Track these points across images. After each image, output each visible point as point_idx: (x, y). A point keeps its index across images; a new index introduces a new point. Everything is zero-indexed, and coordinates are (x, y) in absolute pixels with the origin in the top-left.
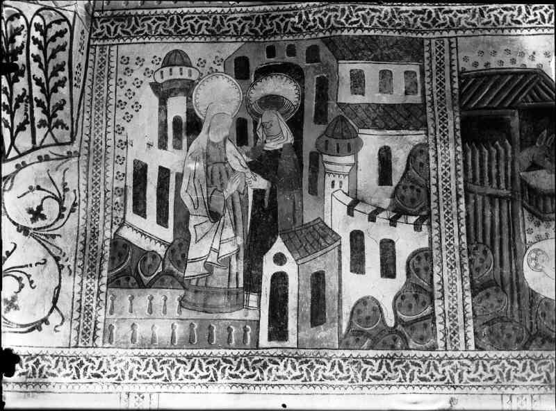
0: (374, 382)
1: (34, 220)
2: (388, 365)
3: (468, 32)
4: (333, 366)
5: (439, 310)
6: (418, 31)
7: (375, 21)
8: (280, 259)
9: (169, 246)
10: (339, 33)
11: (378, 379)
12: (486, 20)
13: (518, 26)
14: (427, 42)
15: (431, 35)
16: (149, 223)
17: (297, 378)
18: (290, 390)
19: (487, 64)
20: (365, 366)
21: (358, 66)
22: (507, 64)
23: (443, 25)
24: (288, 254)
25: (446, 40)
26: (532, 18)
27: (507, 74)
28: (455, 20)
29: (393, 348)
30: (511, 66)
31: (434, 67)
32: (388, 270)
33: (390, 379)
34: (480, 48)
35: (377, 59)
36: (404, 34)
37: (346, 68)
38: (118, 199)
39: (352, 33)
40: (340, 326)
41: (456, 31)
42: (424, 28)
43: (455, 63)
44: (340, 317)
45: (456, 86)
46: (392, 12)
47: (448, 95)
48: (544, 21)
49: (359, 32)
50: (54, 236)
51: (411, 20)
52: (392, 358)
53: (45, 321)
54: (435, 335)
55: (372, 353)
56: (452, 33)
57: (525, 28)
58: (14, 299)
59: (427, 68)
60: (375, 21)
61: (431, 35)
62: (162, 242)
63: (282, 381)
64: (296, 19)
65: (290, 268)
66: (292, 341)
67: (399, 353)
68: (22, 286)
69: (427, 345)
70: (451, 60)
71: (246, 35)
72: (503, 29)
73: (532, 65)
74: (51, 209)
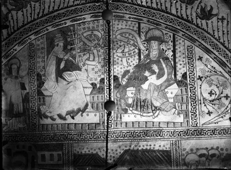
3: (76, 142)
6: (62, 141)
7: (48, 139)
10: (37, 143)
12: (82, 138)
13: (91, 140)
14: (64, 144)
15: (65, 142)
19: (81, 152)
21: (43, 153)
22: (87, 152)
23: (69, 139)
25: (70, 144)
26: (95, 137)
27: (87, 155)
28: (73, 137)
30: (88, 153)
31: (66, 152)
34: (80, 147)
35: (49, 151)
36: (57, 142)
37: (40, 154)
39: (41, 143)
41: (73, 141)
42: (64, 140)
43: (72, 151)
45: (73, 158)
46: (54, 135)
47: (71, 161)
48: (99, 138)
49: (43, 143)
51: (60, 138)
56: (72, 142)
57: (93, 140)
59: (64, 152)
60: (48, 139)
61: (65, 142)
64: (25, 137)
70: (71, 150)
71: (10, 142)
72: (86, 141)
73: (95, 152)
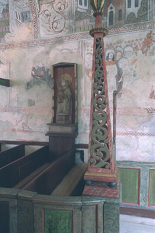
0: (133, 30)
1: (59, 10)
2: (136, 26)
4: (123, 28)
5: (149, 12)
8: (111, 8)
9: (87, 10)
11: (134, 29)
16: (83, 7)
17: (115, 32)
18: (114, 35)
20: (130, 27)
24: (113, 7)
29: (137, 22)
32: (136, 5)
33: (136, 29)
38: (76, 3)
40: (125, 20)
44: (125, 18)
50: (63, 13)
52: (137, 24)
53: (63, 30)
54: (147, 18)
55: (132, 24)
58: (56, 27)
62: (86, 10)
63: (112, 33)
65: (114, 10)
66: (114, 24)
67: (138, 23)
68: (58, 24)
69: (145, 20)
74: (63, 7)
